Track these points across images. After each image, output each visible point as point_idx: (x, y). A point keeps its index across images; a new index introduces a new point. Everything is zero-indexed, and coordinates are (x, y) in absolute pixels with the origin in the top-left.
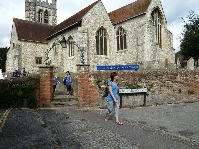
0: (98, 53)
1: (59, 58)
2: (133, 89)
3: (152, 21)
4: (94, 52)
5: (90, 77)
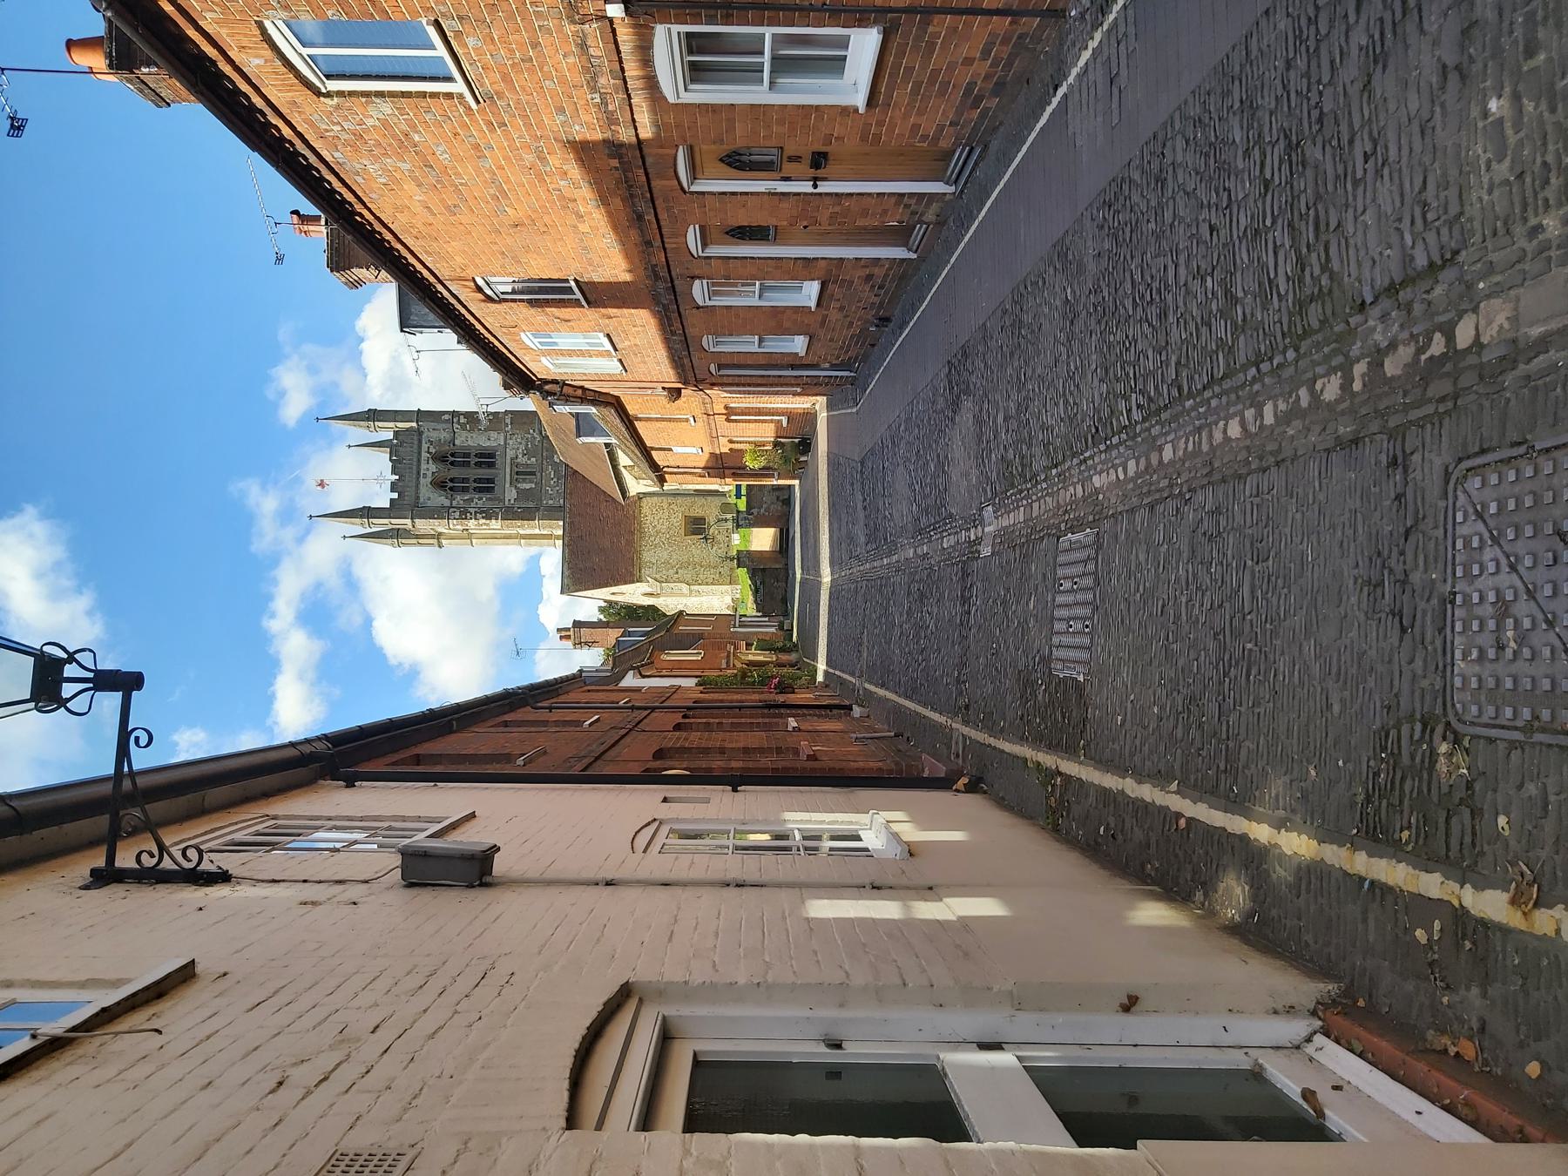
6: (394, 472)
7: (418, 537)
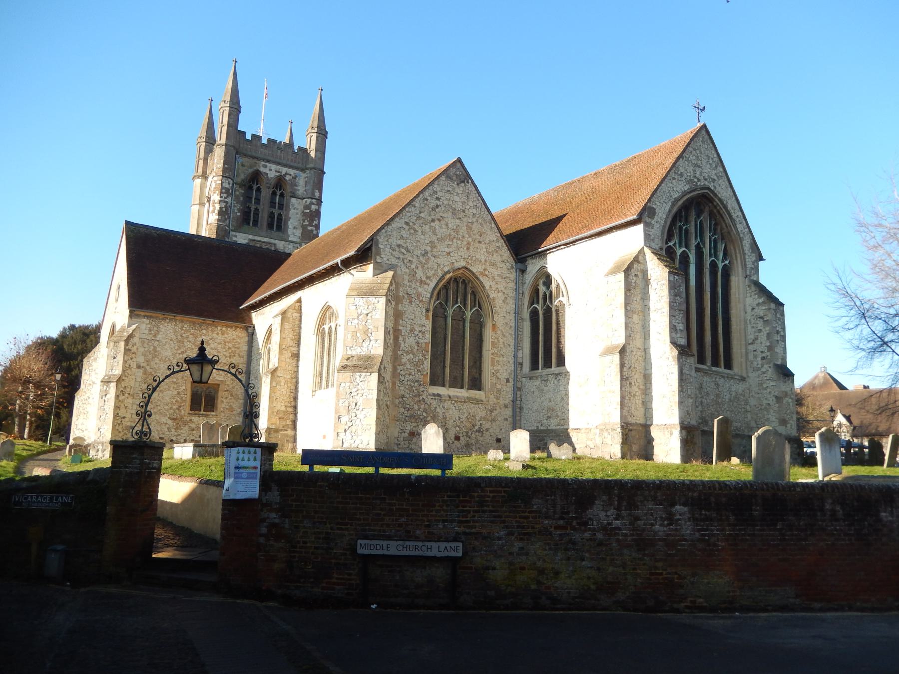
0: (436, 379)
3: (679, 252)
6: (269, 140)
7: (206, 160)
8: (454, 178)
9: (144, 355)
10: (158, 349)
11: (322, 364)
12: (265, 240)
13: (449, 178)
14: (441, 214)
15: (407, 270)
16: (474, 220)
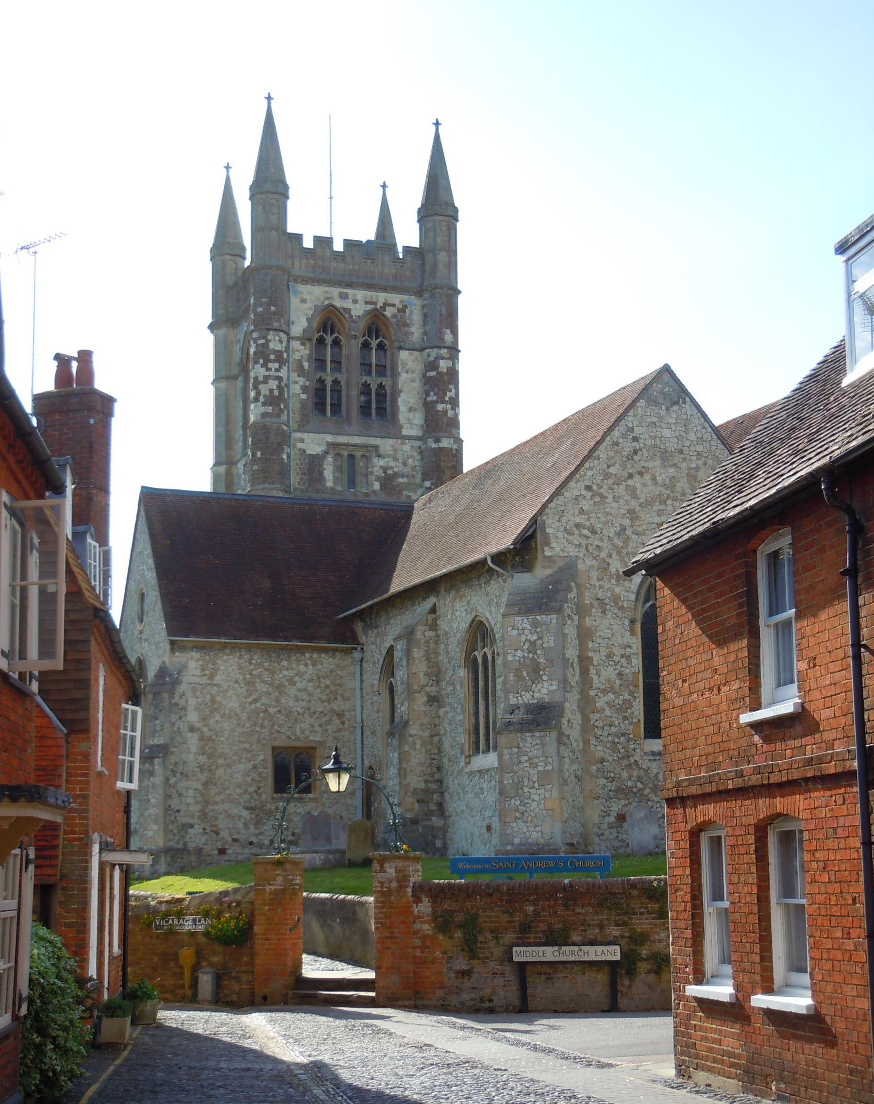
1: (417, 757)
2: (564, 948)
4: (626, 727)
5: (417, 900)
6: (348, 243)
8: (661, 400)
9: (198, 709)
10: (218, 699)
11: (476, 714)
12: (357, 440)
13: (653, 402)
14: (643, 463)
15: (594, 563)
16: (700, 462)
